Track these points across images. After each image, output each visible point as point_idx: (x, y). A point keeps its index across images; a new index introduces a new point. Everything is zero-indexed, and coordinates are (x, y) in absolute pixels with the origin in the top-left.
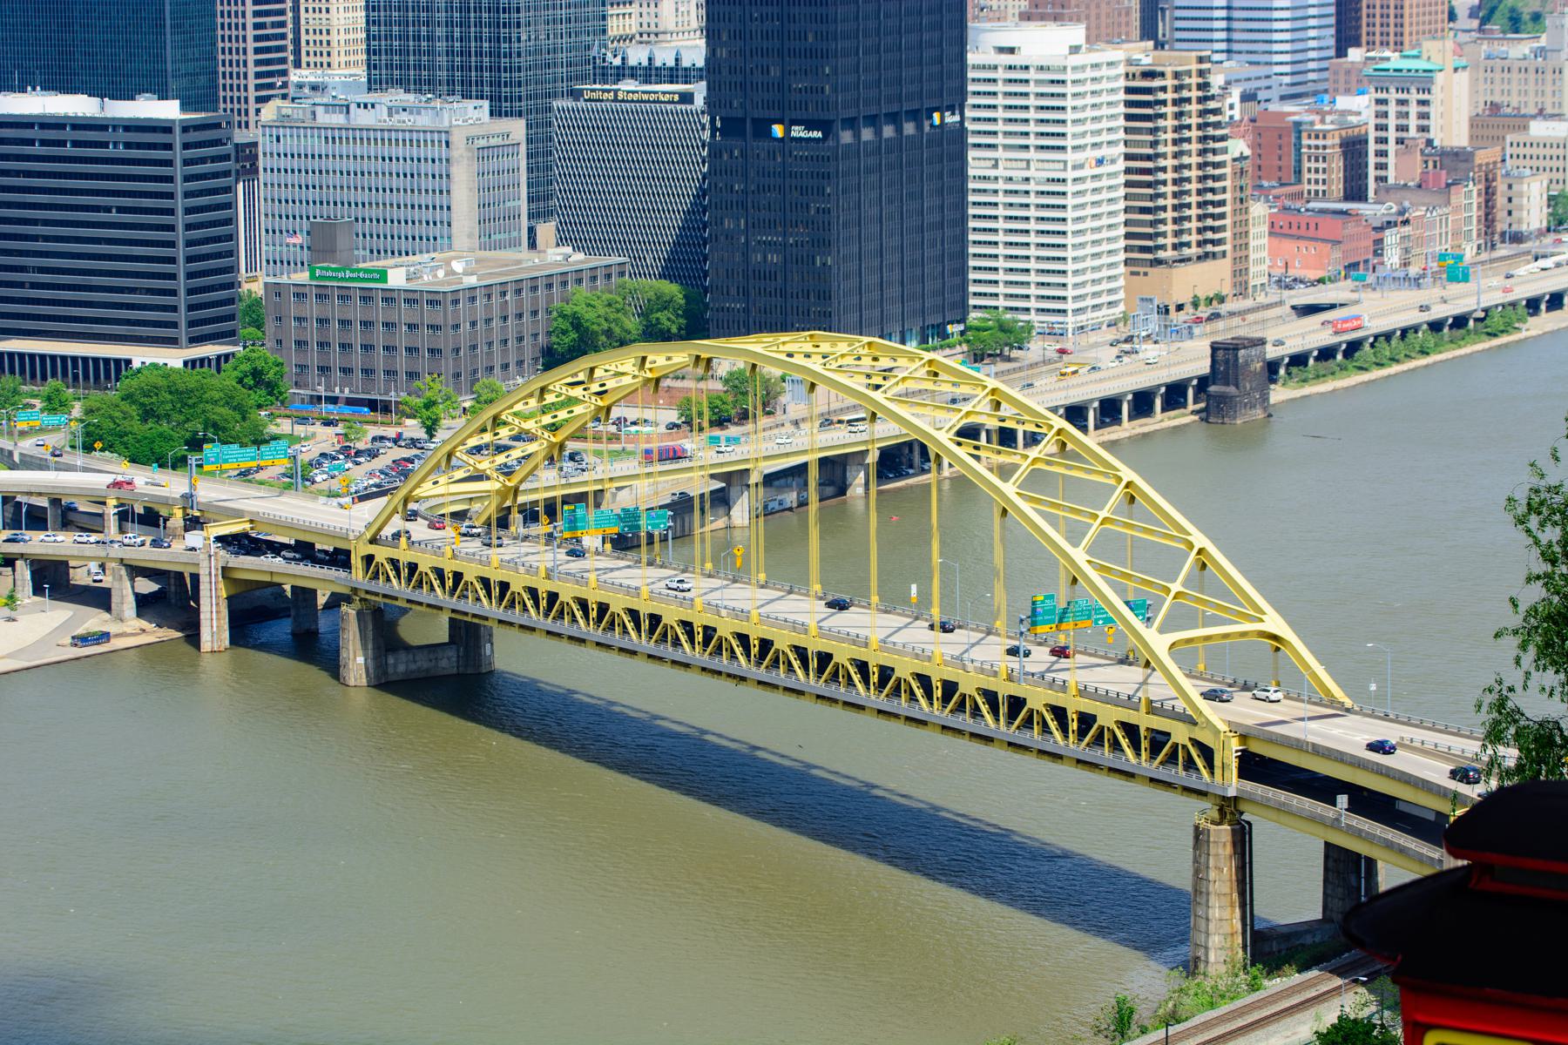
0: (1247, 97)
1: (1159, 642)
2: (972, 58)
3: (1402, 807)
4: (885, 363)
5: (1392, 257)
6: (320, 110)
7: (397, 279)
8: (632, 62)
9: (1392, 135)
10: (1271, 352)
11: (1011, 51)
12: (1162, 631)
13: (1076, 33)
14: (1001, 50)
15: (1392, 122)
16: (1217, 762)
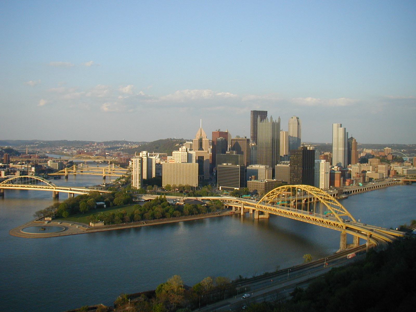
0: (340, 169)
1: (337, 216)
2: (315, 163)
3: (362, 232)
4: (310, 187)
5: (354, 183)
6: (253, 166)
9: (354, 172)
11: (319, 162)
12: (338, 214)
14: (318, 162)
15: (354, 171)
16: (343, 227)
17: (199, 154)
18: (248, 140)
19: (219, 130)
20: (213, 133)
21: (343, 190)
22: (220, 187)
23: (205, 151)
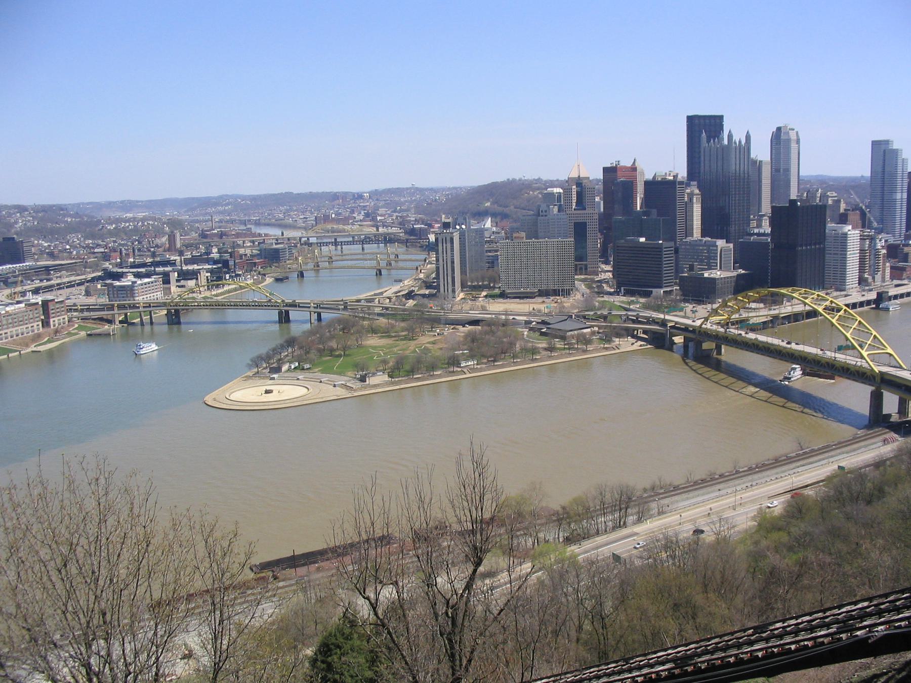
7: (706, 275)
8: (755, 232)
10: (890, 294)
13: (850, 227)
17: (577, 218)
18: (681, 183)
19: (619, 162)
20: (606, 170)
21: (888, 292)
22: (622, 288)
23: (589, 212)
